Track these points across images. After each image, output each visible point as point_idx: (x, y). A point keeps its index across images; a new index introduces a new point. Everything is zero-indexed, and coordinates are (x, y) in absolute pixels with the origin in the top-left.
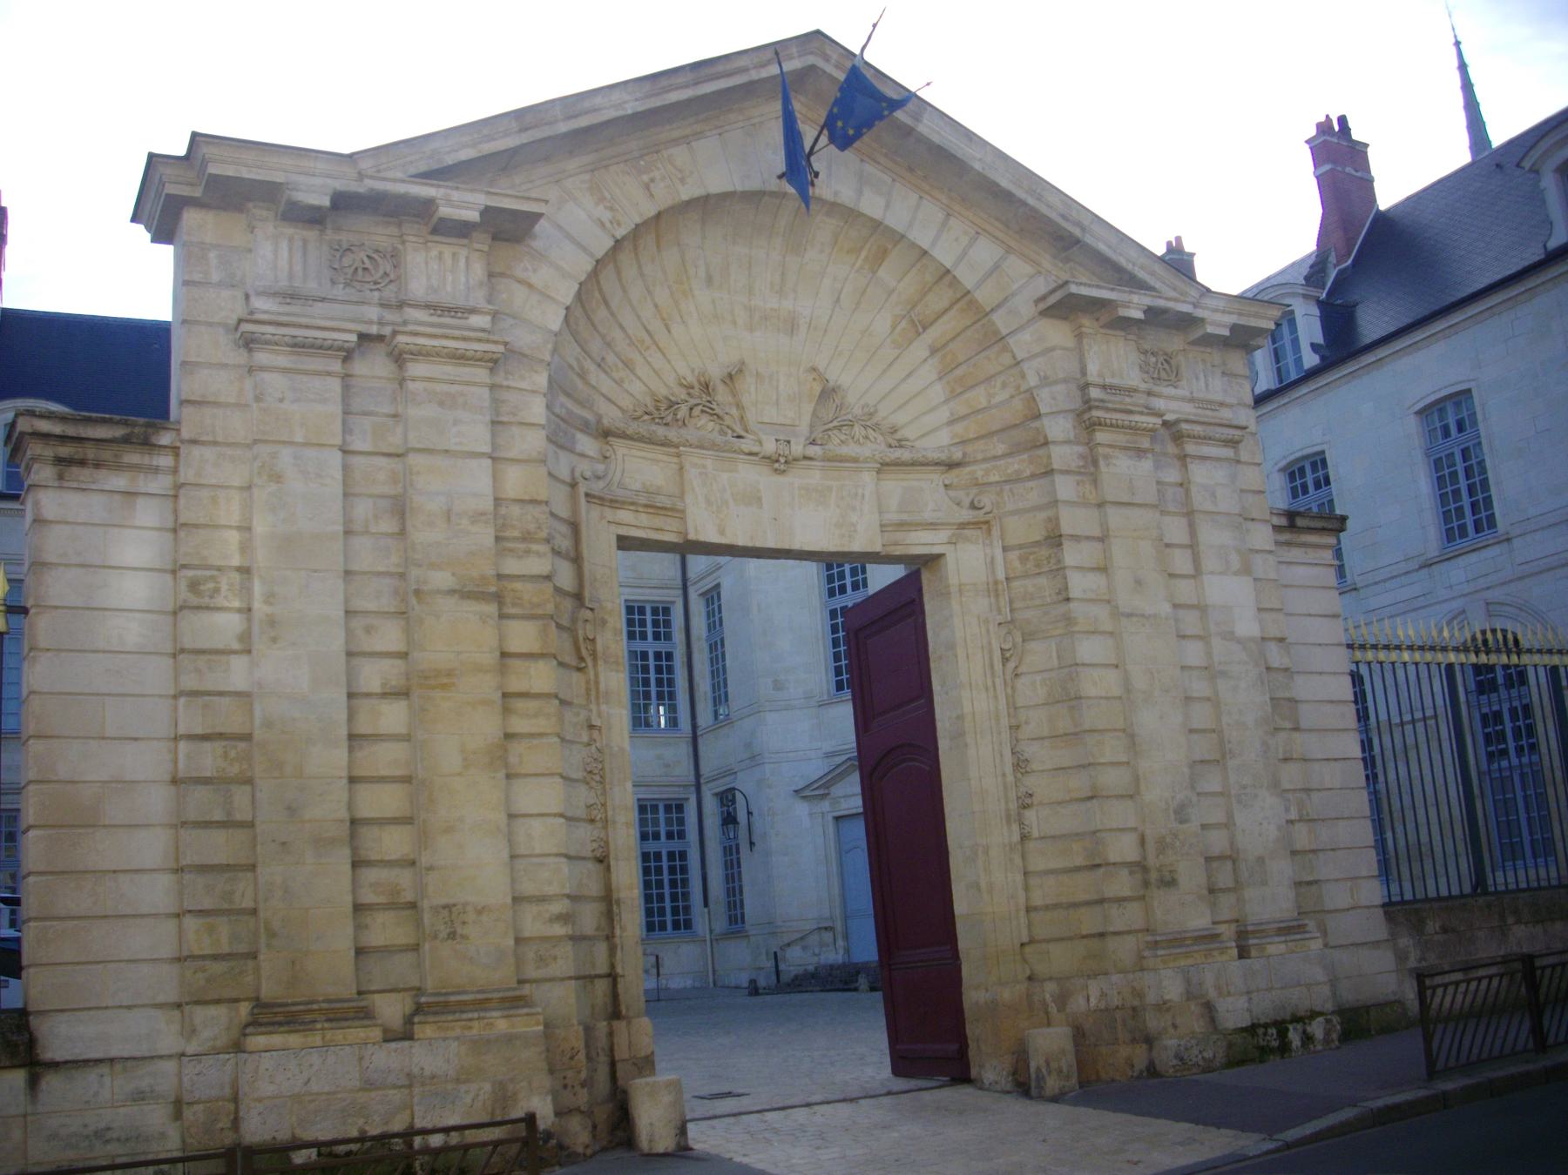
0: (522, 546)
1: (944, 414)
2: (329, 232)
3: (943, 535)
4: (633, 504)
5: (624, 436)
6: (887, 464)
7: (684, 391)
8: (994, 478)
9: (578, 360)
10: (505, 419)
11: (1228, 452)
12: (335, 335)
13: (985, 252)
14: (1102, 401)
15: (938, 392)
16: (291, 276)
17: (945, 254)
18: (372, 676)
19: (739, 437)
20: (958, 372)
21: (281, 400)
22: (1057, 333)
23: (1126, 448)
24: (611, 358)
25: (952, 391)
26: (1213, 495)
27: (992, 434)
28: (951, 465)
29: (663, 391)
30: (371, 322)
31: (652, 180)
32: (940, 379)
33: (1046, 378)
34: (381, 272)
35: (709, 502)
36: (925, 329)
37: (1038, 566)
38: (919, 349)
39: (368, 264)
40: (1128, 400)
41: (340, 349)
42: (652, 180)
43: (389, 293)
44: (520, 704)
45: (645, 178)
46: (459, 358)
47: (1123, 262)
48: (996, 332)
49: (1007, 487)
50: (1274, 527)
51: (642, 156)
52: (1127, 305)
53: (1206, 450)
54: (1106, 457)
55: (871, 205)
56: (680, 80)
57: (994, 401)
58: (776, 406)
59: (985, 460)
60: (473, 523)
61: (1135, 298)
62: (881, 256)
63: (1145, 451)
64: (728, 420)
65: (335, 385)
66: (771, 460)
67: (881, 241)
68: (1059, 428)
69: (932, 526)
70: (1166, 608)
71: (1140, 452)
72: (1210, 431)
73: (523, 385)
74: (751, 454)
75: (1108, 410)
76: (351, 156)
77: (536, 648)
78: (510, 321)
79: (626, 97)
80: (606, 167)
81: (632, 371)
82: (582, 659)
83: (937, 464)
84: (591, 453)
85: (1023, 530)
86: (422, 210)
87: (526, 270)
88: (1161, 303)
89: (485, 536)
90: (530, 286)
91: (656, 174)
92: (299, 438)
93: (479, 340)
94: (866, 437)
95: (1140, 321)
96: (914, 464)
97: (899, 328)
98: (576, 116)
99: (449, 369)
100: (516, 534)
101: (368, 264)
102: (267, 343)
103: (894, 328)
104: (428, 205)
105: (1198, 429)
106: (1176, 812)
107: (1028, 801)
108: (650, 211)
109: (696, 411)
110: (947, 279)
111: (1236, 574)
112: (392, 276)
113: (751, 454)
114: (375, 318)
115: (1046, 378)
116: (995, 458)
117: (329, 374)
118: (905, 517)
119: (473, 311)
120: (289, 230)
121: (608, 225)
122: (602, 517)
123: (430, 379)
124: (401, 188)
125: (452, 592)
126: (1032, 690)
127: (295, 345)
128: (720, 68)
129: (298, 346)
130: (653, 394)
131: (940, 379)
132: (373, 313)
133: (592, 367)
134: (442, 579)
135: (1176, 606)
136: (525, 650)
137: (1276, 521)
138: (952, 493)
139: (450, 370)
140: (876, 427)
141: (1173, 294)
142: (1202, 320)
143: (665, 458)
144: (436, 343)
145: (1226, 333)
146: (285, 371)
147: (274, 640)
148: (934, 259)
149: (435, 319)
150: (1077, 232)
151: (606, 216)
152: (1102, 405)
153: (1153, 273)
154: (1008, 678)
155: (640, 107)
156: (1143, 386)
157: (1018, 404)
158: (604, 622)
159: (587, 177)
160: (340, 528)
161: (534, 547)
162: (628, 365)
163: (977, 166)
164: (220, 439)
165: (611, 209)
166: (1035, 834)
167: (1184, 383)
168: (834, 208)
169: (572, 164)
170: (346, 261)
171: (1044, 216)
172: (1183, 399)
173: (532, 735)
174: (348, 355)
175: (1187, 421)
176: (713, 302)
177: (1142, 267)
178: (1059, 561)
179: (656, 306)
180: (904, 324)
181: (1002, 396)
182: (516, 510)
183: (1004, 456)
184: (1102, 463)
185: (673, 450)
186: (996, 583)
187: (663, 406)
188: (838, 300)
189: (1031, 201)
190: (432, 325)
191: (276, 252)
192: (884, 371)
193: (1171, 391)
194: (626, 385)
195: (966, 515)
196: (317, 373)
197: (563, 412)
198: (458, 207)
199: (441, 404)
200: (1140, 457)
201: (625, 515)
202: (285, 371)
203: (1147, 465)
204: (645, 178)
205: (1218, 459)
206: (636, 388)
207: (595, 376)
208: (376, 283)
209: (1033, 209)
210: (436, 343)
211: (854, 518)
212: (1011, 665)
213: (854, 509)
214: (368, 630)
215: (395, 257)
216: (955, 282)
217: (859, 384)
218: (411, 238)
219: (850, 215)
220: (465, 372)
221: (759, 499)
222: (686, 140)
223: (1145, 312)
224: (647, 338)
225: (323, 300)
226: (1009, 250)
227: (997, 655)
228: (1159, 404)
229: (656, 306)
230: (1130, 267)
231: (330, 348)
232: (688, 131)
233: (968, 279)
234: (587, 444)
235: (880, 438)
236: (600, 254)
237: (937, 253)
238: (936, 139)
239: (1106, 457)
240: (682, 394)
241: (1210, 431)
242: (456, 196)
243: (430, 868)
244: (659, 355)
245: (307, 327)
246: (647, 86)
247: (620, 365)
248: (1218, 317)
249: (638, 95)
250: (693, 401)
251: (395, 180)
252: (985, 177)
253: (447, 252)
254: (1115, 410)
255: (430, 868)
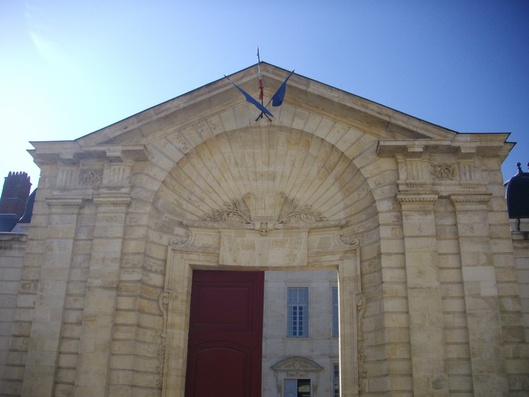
0: (131, 270)
1: (342, 205)
2: (81, 167)
3: (337, 257)
4: (196, 252)
5: (194, 227)
6: (313, 229)
7: (226, 207)
8: (361, 230)
9: (176, 200)
10: (132, 224)
11: (484, 207)
12: (74, 201)
13: (353, 135)
14: (407, 191)
15: (339, 196)
16: (66, 182)
17: (331, 139)
18: (73, 317)
19: (248, 223)
20: (347, 187)
21: (57, 224)
22: (386, 164)
23: (417, 211)
24: (193, 198)
25: (345, 195)
26: (472, 228)
27: (361, 211)
28: (342, 227)
29: (218, 208)
30: (89, 195)
31: (202, 131)
32: (340, 190)
33: (379, 184)
34: (95, 178)
35: (230, 250)
36: (332, 171)
37: (374, 268)
38: (331, 179)
39: (91, 176)
40: (420, 189)
41: (77, 205)
42: (202, 131)
43: (97, 184)
44: (122, 328)
45: (200, 130)
46: (115, 204)
47: (411, 128)
48: (356, 167)
49: (365, 234)
50: (513, 240)
51: (199, 122)
52: (413, 146)
53: (468, 207)
54: (406, 216)
55: (298, 124)
56: (202, 92)
57: (361, 197)
58: (264, 208)
59: (358, 223)
60: (112, 262)
61: (417, 143)
62: (308, 145)
63: (430, 211)
64: (245, 217)
65: (75, 217)
66: (260, 231)
67: (306, 138)
68: (384, 206)
69: (332, 253)
70: (436, 284)
71: (426, 212)
72: (469, 198)
73: (141, 211)
74: (251, 229)
75: (406, 194)
76: (76, 140)
77: (131, 307)
78: (140, 189)
79: (180, 102)
80: (184, 129)
81: (204, 202)
82: (162, 312)
83: (335, 226)
84: (182, 234)
85: (369, 252)
86: (102, 156)
87: (148, 170)
88: (432, 143)
89: (115, 267)
90: (149, 176)
91: (204, 128)
92: (60, 236)
93: (121, 197)
94: (307, 218)
95: (421, 153)
96: (324, 227)
97: (321, 172)
98: (160, 113)
99: (112, 208)
100: (130, 265)
101: (91, 176)
102: (54, 205)
103: (319, 172)
104: (104, 152)
105: (461, 198)
106: (433, 383)
107: (364, 375)
108: (199, 141)
109: (231, 215)
110: (334, 149)
111: (483, 265)
112: (99, 179)
113: (251, 229)
114: (91, 194)
115: (379, 184)
116: (362, 221)
117: (73, 214)
118: (320, 250)
119: (122, 187)
120: (67, 168)
121: (182, 150)
122: (182, 258)
123: (104, 212)
124: (94, 149)
125: (100, 287)
126: (369, 324)
127: (63, 205)
128: (219, 84)
129: (65, 205)
130: (213, 210)
131: (340, 190)
132: (90, 191)
133: (184, 202)
134: (98, 282)
135: (442, 283)
136: (127, 308)
137: (515, 237)
138: (343, 238)
139: (112, 208)
140: (311, 214)
141: (439, 138)
142: (459, 147)
143: (215, 234)
144: (106, 200)
145: (474, 151)
146: (59, 214)
147: (41, 304)
148: (327, 142)
149: (109, 191)
150: (387, 119)
151: (181, 146)
152: (406, 192)
153: (427, 130)
154: (359, 318)
155: (186, 105)
156: (428, 182)
157: (369, 197)
158: (176, 297)
159: (177, 133)
160: (68, 266)
161: (136, 270)
162: (202, 200)
163: (336, 100)
164: (39, 238)
165: (184, 144)
166: (367, 390)
167: (457, 177)
168: (281, 128)
169: (171, 130)
170: (85, 175)
171: (370, 115)
172: (455, 185)
173: (125, 340)
174: (81, 207)
175: (454, 195)
176: (239, 172)
177: (421, 129)
178: (381, 265)
179: (214, 177)
180: (323, 170)
181: (363, 195)
182: (131, 257)
183: (365, 220)
184: (404, 219)
185: (217, 231)
186: (357, 276)
187: (216, 214)
188: (294, 164)
189: (362, 110)
190: (108, 194)
191: (63, 176)
192: (316, 190)
193: (449, 182)
194: (201, 208)
195: (348, 247)
196: (69, 214)
197: (167, 219)
198: (113, 152)
199: (107, 221)
200: (426, 214)
201: (194, 256)
202: (59, 214)
203: (430, 217)
204: (200, 130)
205: (475, 211)
206: (206, 209)
207: (185, 205)
208: (93, 182)
209: (366, 113)
210: (106, 200)
211: (296, 252)
212: (361, 313)
213: (296, 248)
214: (75, 301)
215: (102, 171)
216: (337, 150)
217: (303, 196)
218: (106, 165)
219: (290, 130)
220: (118, 208)
221: (254, 247)
222: (218, 113)
223: (423, 148)
224: (211, 190)
225: (74, 189)
226: (365, 132)
227: (355, 307)
228: (438, 188)
229: (214, 177)
230: (415, 129)
231: (74, 205)
232: (218, 110)
233: (341, 147)
234: (180, 231)
235: (313, 218)
236: (177, 160)
237: (328, 139)
238: (316, 93)
239: (406, 216)
240: (226, 208)
241: (469, 198)
242: (112, 148)
243: (77, 386)
244: (216, 195)
245: (65, 199)
246: (188, 97)
247: (198, 200)
248: (468, 145)
249: (185, 101)
250: (230, 211)
251: (92, 146)
252: (340, 104)
253: (117, 168)
254: (410, 194)
255: (77, 386)
